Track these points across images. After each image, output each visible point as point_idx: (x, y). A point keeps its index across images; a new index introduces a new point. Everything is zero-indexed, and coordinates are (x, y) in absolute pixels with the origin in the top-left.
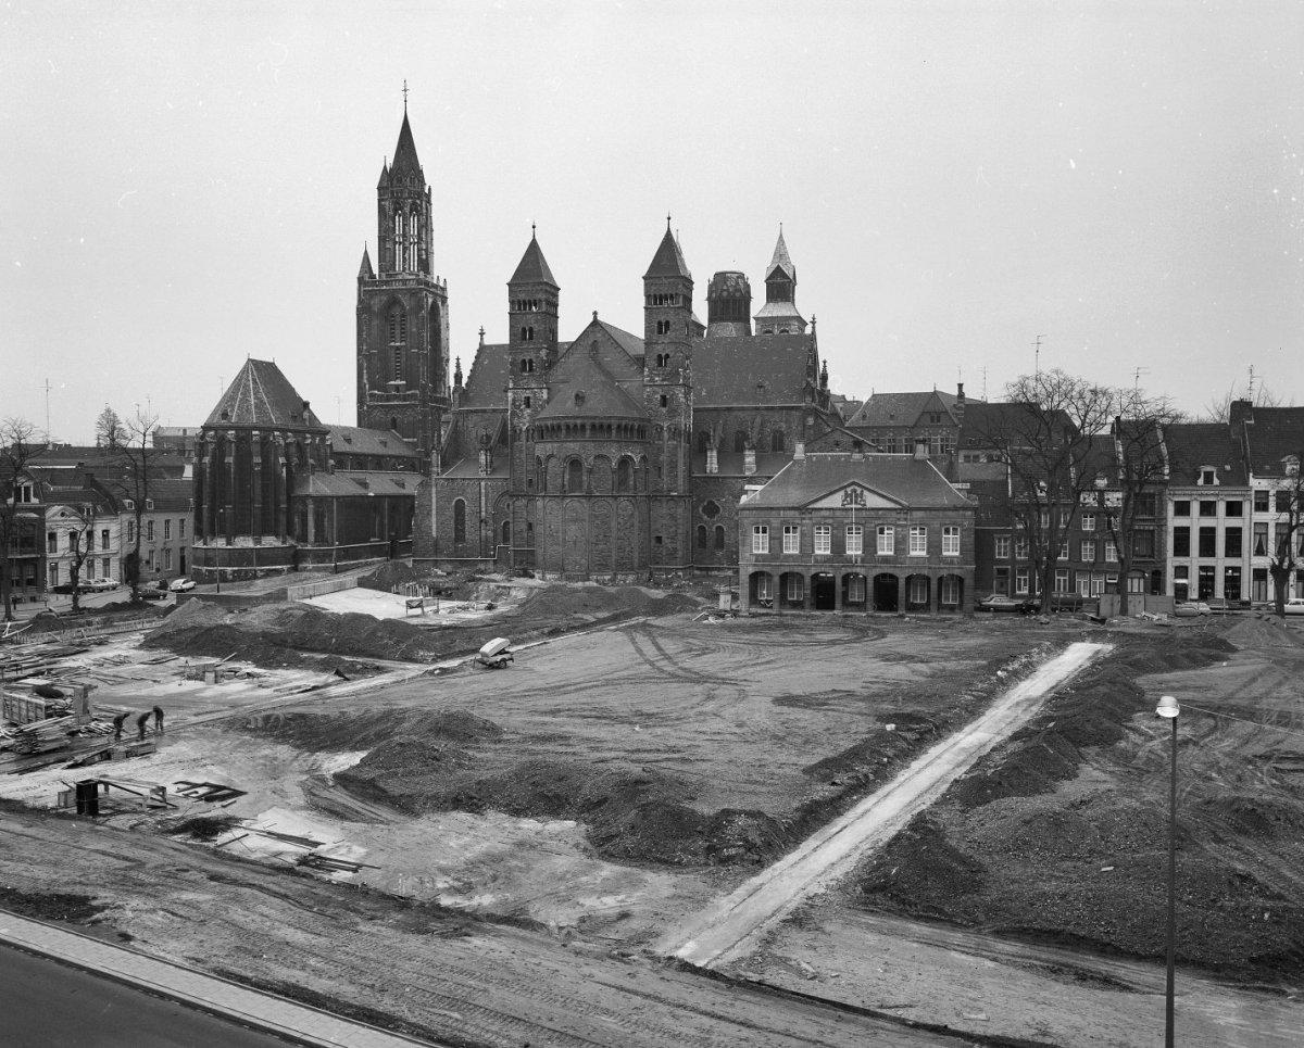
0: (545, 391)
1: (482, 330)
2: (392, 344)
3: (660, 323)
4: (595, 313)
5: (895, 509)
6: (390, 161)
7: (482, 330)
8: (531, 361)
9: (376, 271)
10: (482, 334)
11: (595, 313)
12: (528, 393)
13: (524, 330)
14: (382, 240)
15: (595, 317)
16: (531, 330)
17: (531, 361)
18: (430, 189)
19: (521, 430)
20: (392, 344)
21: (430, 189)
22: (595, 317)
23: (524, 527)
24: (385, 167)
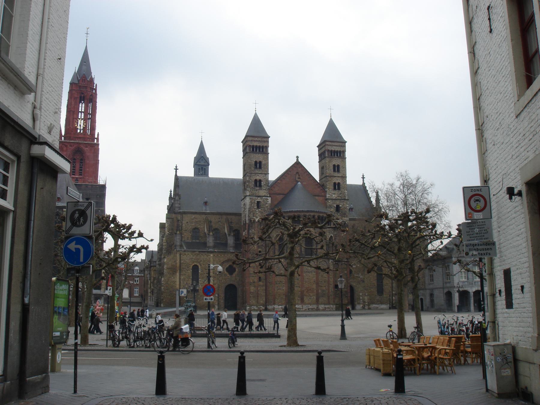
0: (269, 199)
1: (176, 167)
3: (334, 166)
4: (297, 157)
7: (176, 167)
8: (260, 181)
10: (176, 169)
11: (297, 157)
12: (259, 199)
13: (256, 162)
15: (297, 160)
16: (260, 162)
17: (260, 181)
19: (254, 221)
22: (297, 160)
23: (256, 279)
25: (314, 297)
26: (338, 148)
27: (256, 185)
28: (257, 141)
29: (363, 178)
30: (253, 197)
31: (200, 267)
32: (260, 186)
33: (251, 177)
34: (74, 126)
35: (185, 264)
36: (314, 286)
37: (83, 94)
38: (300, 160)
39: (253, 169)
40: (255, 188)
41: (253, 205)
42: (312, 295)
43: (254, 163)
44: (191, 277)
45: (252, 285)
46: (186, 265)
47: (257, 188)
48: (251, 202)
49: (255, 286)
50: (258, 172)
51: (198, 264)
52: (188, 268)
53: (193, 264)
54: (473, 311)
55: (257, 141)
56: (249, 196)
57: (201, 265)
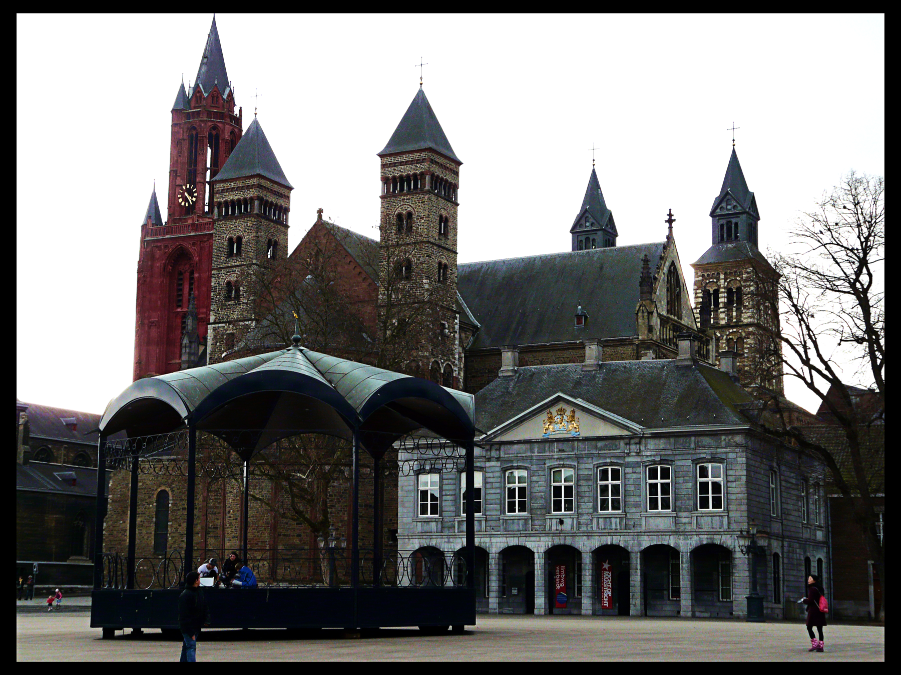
2: (179, 310)
4: (320, 211)
5: (621, 438)
6: (190, 82)
9: (164, 218)
11: (320, 211)
13: (231, 240)
14: (173, 174)
15: (320, 217)
16: (239, 239)
18: (240, 111)
20: (179, 310)
21: (240, 111)
22: (320, 217)
24: (183, 87)
25: (265, 562)
26: (409, 167)
27: (228, 297)
28: (233, 189)
29: (670, 221)
30: (220, 325)
31: (170, 493)
32: (238, 297)
33: (219, 277)
34: (176, 202)
35: (145, 488)
36: (266, 536)
37: (195, 128)
38: (325, 218)
39: (223, 257)
40: (227, 303)
41: (218, 344)
42: (258, 558)
43: (226, 243)
44: (154, 520)
45: (212, 534)
46: (146, 490)
47: (230, 303)
48: (215, 337)
49: (216, 537)
50: (233, 264)
51: (167, 489)
52: (150, 498)
53: (159, 490)
54: (542, 611)
55: (233, 189)
56: (215, 323)
57: (173, 491)
